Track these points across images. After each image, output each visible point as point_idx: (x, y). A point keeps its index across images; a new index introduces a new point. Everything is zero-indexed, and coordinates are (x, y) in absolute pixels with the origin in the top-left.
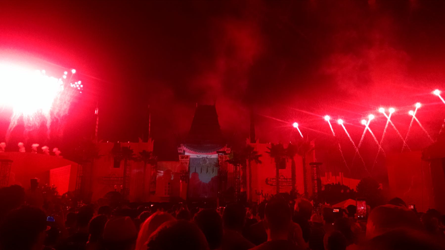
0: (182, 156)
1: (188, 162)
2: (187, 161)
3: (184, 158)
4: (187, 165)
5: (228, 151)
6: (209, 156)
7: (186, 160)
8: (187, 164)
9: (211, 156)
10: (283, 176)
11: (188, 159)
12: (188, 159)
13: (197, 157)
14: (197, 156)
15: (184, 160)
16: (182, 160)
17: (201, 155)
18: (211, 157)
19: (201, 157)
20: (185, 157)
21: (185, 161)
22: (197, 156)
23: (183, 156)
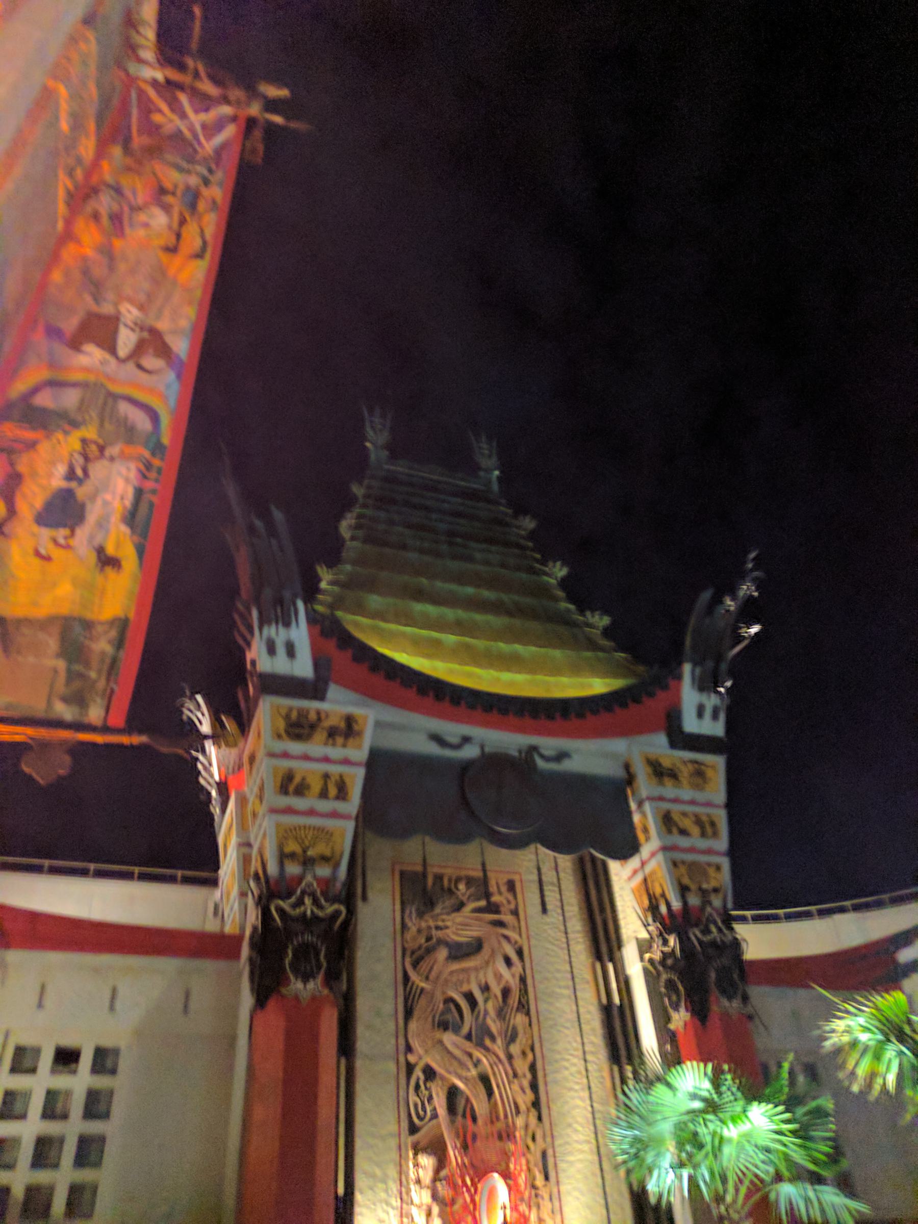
0: (294, 715)
1: (361, 772)
2: (346, 762)
3: (320, 736)
4: (341, 807)
6: (549, 744)
7: (335, 752)
8: (342, 793)
11: (359, 747)
12: (359, 747)
13: (433, 749)
15: (316, 747)
16: (295, 747)
17: (477, 732)
18: (568, 766)
19: (470, 752)
20: (327, 724)
21: (326, 760)
22: (437, 739)
23: (303, 714)
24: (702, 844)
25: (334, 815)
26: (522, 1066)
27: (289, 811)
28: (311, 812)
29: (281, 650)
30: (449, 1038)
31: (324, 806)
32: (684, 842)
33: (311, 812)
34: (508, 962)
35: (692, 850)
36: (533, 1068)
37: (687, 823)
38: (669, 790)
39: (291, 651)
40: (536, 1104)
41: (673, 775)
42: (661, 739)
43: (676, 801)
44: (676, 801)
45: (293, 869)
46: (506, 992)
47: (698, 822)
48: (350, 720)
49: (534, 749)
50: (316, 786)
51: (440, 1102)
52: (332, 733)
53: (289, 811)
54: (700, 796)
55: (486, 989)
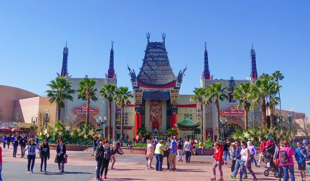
1: (142, 95)
5: (178, 85)
6: (161, 89)
8: (141, 96)
9: (163, 90)
10: (234, 109)
13: (150, 91)
14: (150, 90)
16: (137, 93)
17: (154, 89)
18: (163, 91)
19: (153, 91)
21: (139, 94)
24: (175, 99)
25: (140, 99)
26: (160, 115)
27: (137, 99)
28: (138, 99)
29: (135, 84)
30: (154, 113)
31: (139, 98)
32: (173, 98)
33: (138, 99)
34: (160, 106)
35: (174, 99)
36: (161, 115)
37: (174, 97)
38: (173, 94)
39: (136, 84)
40: (161, 118)
41: (174, 92)
42: (173, 88)
43: (174, 94)
44: (174, 94)
45: (137, 103)
46: (159, 109)
47: (175, 96)
48: (141, 90)
49: (160, 90)
50: (139, 97)
51: (153, 118)
52: (140, 91)
53: (137, 99)
54: (176, 94)
55: (158, 108)
